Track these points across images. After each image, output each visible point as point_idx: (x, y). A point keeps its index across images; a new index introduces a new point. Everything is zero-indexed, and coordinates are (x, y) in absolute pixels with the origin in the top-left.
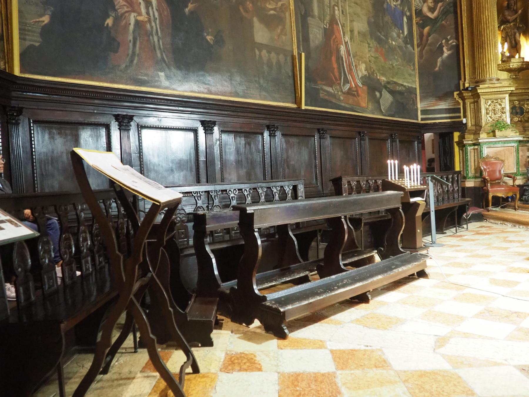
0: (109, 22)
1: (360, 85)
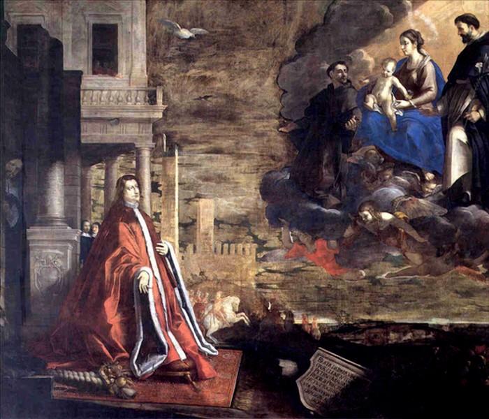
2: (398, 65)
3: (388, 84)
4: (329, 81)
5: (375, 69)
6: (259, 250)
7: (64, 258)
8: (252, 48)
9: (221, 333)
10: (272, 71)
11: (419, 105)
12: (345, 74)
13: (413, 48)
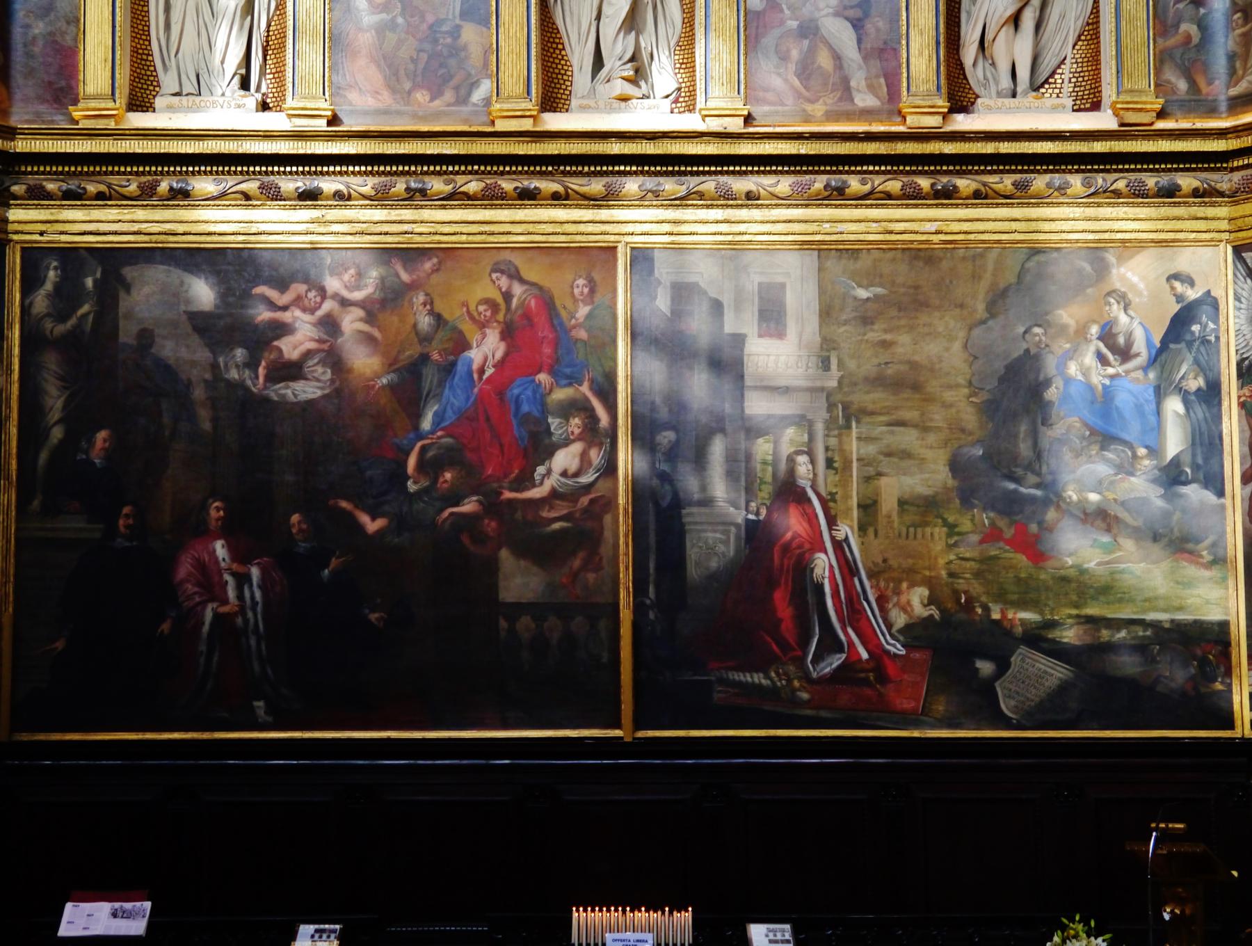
0: (166, 627)
1: (897, 649)
2: (1103, 328)
3: (1092, 348)
4: (1025, 346)
5: (1077, 332)
6: (949, 535)
7: (726, 543)
8: (938, 308)
9: (907, 629)
10: (962, 334)
11: (1127, 372)
12: (1043, 338)
13: (1119, 309)
